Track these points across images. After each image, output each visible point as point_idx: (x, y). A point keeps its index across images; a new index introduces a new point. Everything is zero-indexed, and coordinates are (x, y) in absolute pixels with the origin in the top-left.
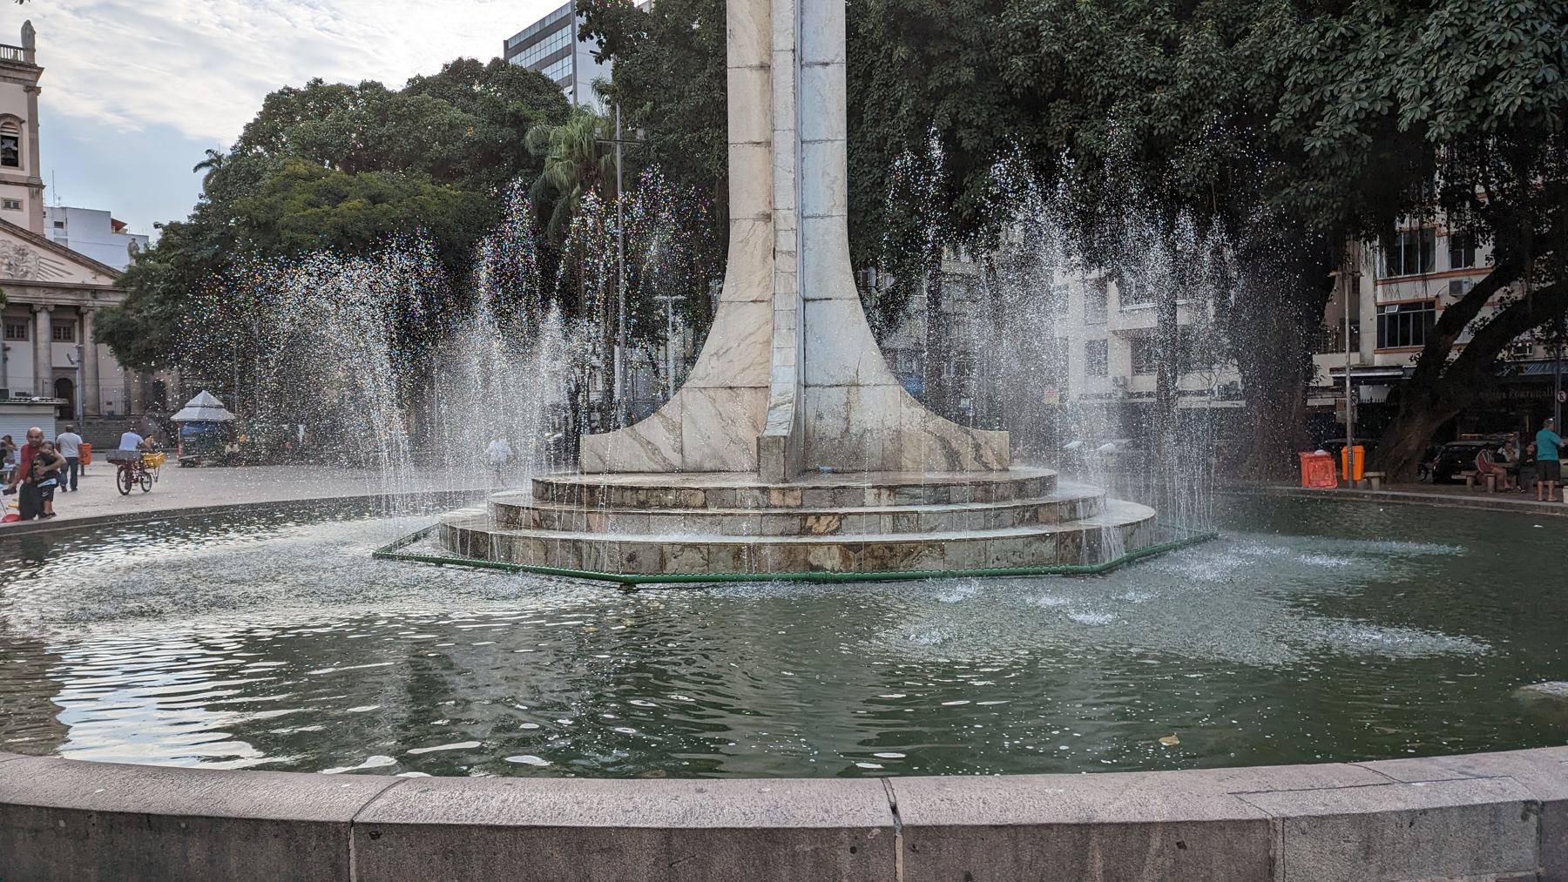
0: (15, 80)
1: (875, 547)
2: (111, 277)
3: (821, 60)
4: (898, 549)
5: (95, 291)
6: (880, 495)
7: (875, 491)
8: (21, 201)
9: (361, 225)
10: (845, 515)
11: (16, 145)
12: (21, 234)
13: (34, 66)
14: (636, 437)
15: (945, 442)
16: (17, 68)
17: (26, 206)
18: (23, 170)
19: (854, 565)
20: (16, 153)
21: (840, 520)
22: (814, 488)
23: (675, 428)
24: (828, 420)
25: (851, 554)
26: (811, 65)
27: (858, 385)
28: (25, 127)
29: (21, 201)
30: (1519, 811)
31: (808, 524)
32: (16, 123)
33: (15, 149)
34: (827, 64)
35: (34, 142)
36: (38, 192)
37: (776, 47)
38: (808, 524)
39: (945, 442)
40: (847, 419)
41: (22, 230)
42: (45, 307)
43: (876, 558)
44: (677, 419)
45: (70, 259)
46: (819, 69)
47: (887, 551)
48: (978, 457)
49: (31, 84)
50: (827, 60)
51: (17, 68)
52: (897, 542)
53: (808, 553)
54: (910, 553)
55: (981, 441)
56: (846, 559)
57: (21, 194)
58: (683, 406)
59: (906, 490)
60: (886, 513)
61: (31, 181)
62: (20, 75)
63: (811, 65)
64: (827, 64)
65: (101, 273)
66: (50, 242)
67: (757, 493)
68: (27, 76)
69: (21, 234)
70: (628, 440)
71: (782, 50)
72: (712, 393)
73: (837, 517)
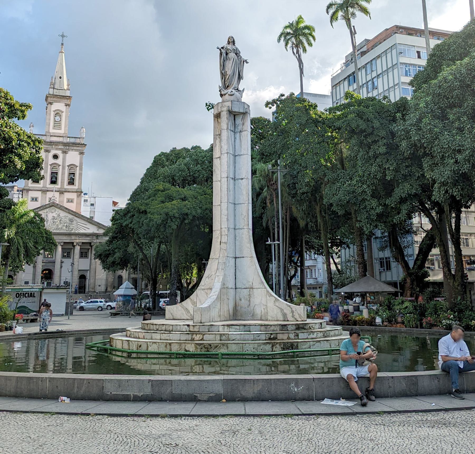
0: (76, 150)
1: (205, 344)
2: (104, 229)
3: (241, 178)
4: (212, 345)
5: (97, 236)
6: (224, 328)
7: (223, 327)
8: (74, 199)
9: (175, 211)
10: (205, 334)
11: (74, 176)
12: (72, 213)
14: (183, 307)
15: (282, 310)
17: (75, 201)
18: (75, 186)
19: (199, 350)
20: (73, 179)
21: (203, 336)
22: (203, 325)
23: (194, 304)
24: (243, 300)
25: (198, 346)
26: (238, 179)
27: (253, 288)
28: (78, 168)
29: (74, 199)
30: (148, 381)
31: (193, 337)
32: (75, 167)
33: (73, 178)
34: (242, 179)
35: (81, 175)
36: (80, 195)
38: (193, 337)
39: (282, 310)
40: (249, 301)
41: (72, 211)
42: (77, 244)
43: (206, 348)
44: (195, 300)
45: (89, 222)
46: (240, 180)
47: (209, 346)
48: (293, 316)
49: (82, 151)
50: (243, 178)
51: (77, 145)
52: (212, 343)
53: (185, 346)
54: (217, 347)
55: (294, 310)
56: (196, 348)
57: (73, 196)
58: (197, 296)
59: (234, 327)
60: (218, 334)
61: (78, 190)
62: (78, 148)
63: (238, 179)
64: (242, 179)
65: (100, 228)
66: (82, 216)
67: (186, 326)
68: (80, 148)
69: (72, 213)
70: (180, 308)
72: (206, 291)
73: (202, 335)
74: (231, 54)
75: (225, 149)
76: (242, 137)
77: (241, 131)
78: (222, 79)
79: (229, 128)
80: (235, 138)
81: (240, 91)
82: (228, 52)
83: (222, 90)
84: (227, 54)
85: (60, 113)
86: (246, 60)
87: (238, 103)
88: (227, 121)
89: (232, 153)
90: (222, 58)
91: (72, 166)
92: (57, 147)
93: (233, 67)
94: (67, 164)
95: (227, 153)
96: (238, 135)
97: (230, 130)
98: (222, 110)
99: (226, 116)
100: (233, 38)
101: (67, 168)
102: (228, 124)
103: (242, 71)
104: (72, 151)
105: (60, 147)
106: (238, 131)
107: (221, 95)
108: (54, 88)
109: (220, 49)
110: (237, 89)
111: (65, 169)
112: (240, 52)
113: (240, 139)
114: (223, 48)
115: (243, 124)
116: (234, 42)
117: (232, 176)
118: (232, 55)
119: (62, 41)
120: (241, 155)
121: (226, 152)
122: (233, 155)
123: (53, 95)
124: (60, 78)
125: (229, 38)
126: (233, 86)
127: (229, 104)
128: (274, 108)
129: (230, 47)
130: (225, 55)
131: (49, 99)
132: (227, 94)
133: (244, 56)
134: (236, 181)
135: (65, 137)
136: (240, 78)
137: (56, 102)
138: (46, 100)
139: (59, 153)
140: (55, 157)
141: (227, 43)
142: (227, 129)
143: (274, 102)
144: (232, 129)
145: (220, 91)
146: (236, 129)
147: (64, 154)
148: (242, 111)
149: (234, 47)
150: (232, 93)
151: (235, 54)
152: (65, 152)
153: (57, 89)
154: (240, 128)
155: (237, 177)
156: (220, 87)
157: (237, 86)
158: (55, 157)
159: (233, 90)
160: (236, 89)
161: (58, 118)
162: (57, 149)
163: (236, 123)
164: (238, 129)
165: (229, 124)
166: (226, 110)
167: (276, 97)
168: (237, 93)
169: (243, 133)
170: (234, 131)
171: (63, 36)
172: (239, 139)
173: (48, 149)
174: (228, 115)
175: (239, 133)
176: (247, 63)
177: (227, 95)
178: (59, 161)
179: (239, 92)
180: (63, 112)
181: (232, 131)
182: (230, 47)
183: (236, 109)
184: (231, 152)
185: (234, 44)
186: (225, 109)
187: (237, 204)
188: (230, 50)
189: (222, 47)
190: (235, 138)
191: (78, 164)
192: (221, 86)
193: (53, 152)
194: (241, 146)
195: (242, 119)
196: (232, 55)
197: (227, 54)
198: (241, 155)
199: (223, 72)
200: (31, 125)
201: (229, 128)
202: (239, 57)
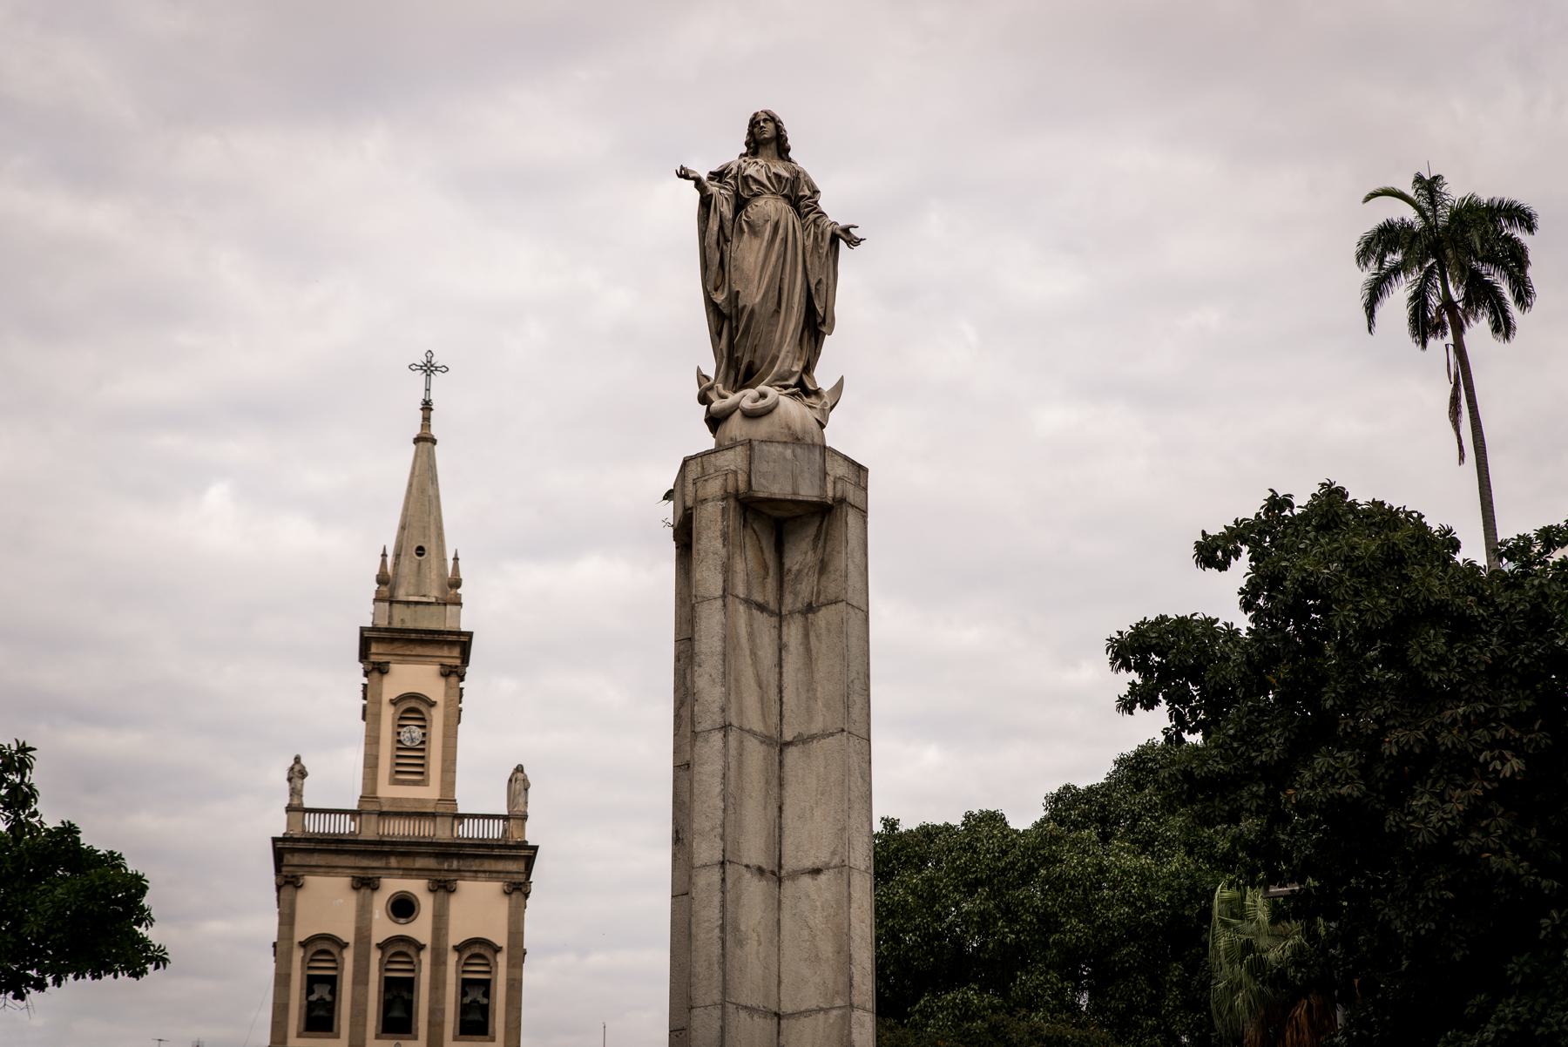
0: (492, 875)
3: (808, 863)
11: (487, 994)
13: (523, 845)
16: (496, 852)
26: (795, 875)
28: (502, 959)
33: (485, 1001)
34: (816, 872)
35: (515, 986)
37: (697, 862)
46: (806, 881)
50: (819, 864)
51: (496, 852)
62: (500, 866)
64: (816, 872)
71: (705, 866)
74: (761, 202)
75: (716, 708)
76: (818, 636)
77: (810, 609)
78: (719, 334)
79: (741, 590)
80: (781, 648)
81: (817, 393)
82: (745, 194)
83: (712, 395)
84: (740, 204)
85: (423, 708)
86: (846, 230)
87: (789, 453)
88: (723, 552)
89: (758, 726)
90: (714, 225)
91: (477, 949)
92: (407, 863)
93: (770, 268)
94: (456, 936)
95: (725, 728)
96: (793, 633)
97: (748, 602)
98: (701, 494)
99: (719, 526)
100: (772, 118)
101: (452, 959)
102: (727, 570)
103: (823, 287)
104: (475, 879)
105: (420, 863)
106: (799, 605)
107: (715, 422)
108: (392, 602)
109: (699, 183)
110: (800, 384)
111: (445, 963)
112: (816, 192)
113: (808, 650)
114: (718, 176)
115: (823, 567)
116: (780, 146)
117: (754, 850)
118: (769, 207)
119: (428, 390)
120: (812, 738)
121: (719, 720)
122: (766, 740)
123: (386, 630)
124: (420, 551)
125: (754, 123)
126: (776, 369)
127: (733, 460)
128: (1241, 568)
129: (756, 169)
130: (727, 210)
131: (374, 648)
132: (738, 413)
133: (834, 206)
134: (787, 884)
135: (443, 815)
136: (815, 326)
137: (404, 659)
138: (364, 655)
139: (416, 887)
140: (403, 907)
141: (744, 149)
142: (724, 597)
143: (1239, 533)
144: (758, 597)
145: (703, 399)
146: (788, 599)
147: (441, 893)
148: (808, 491)
149: (780, 168)
150: (761, 403)
151: (783, 205)
152: (443, 887)
153: (408, 603)
154: (805, 589)
155: (789, 864)
156: (702, 377)
157: (797, 368)
158: (403, 907)
159: (773, 393)
160: (792, 381)
161: (412, 733)
162: (408, 873)
163: (786, 567)
164: (796, 594)
165: (739, 566)
166: (720, 493)
167: (1251, 508)
168: (792, 409)
169: (823, 617)
170: (773, 605)
171: (429, 368)
172: (801, 649)
173: (370, 874)
174: (734, 520)
175: (798, 618)
176: (853, 242)
177: (737, 415)
178: (420, 929)
179: (813, 400)
180: (432, 704)
181: (762, 608)
182: (756, 169)
183: (774, 485)
184: (754, 721)
185: (783, 151)
186: (714, 487)
187: (792, 1015)
188: (756, 181)
189: (715, 168)
190: (781, 648)
191: (501, 939)
192: (710, 372)
193: (392, 886)
194: (810, 687)
195: (817, 537)
196: (769, 207)
197: (740, 204)
198: (812, 738)
199: (720, 298)
200: (297, 768)
201: (741, 590)
202: (812, 216)
